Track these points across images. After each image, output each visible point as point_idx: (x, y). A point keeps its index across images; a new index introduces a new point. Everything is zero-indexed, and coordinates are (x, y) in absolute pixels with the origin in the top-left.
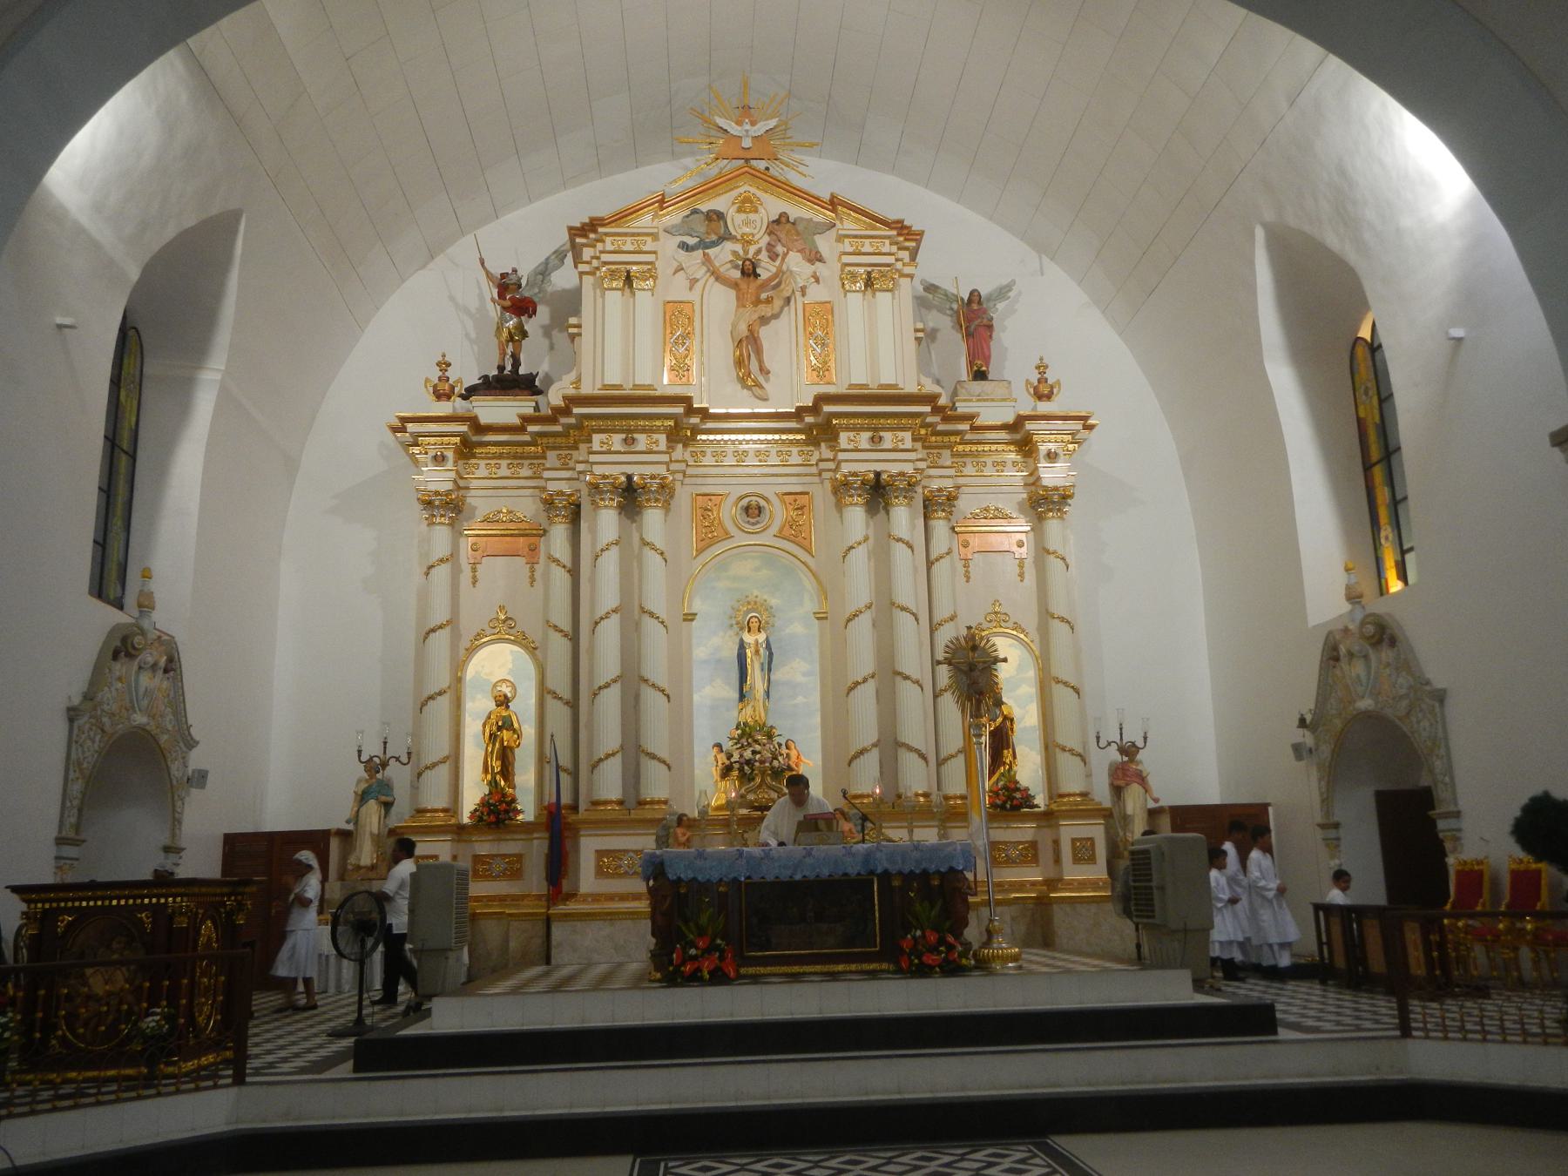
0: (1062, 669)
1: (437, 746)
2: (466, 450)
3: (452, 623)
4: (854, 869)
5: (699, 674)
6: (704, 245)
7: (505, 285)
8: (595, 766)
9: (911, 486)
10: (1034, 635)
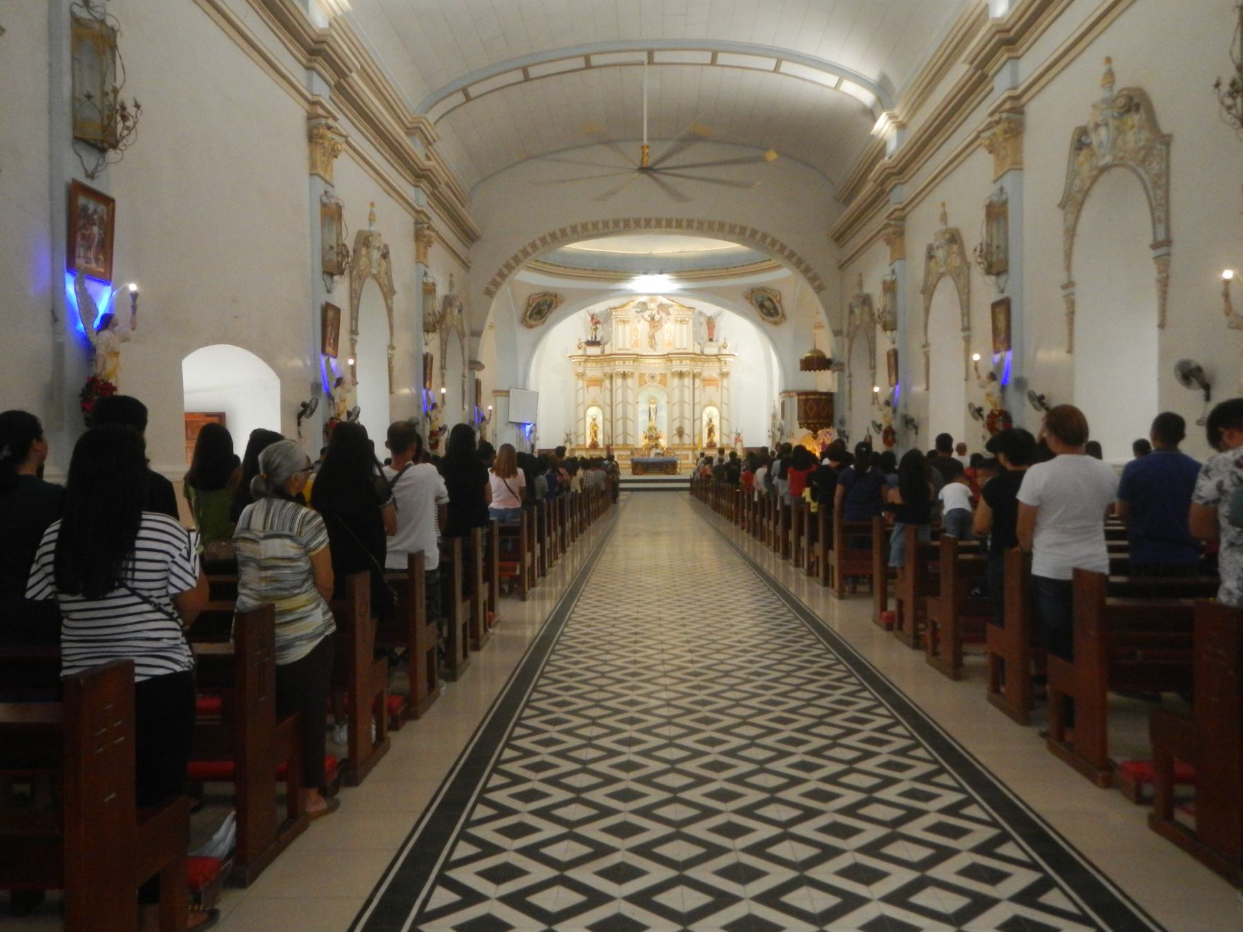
0: (724, 415)
1: (581, 431)
2: (586, 361)
3: (583, 403)
4: (661, 461)
5: (640, 414)
6: (641, 311)
7: (593, 317)
8: (617, 437)
9: (689, 374)
10: (719, 405)
